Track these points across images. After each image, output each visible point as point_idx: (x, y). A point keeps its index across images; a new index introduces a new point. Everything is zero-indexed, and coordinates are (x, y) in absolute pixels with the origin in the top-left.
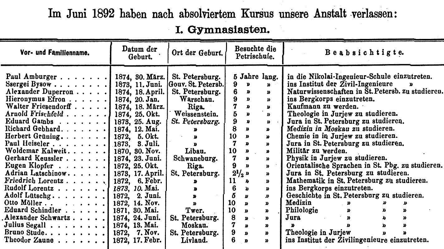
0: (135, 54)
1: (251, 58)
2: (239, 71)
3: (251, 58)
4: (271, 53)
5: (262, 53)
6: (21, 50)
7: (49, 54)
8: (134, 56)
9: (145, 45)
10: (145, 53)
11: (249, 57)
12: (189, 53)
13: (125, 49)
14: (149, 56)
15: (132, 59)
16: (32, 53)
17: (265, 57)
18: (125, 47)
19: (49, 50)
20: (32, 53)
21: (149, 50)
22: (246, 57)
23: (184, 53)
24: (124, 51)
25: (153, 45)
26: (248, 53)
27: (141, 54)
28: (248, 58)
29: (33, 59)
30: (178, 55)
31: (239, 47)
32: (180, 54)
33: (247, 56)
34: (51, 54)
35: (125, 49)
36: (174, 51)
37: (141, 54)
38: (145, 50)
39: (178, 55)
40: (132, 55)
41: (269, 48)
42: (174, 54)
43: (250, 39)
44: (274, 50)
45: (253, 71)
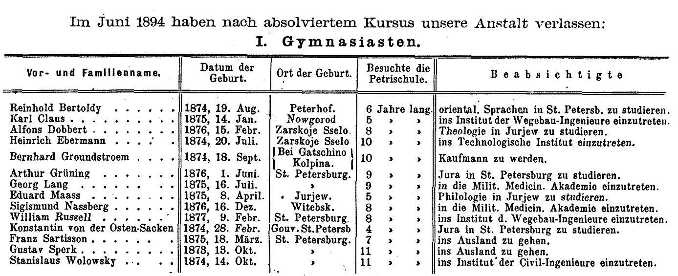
0: (219, 74)
1: (392, 82)
2: (375, 101)
6: (28, 70)
7: (84, 75)
8: (217, 77)
9: (235, 63)
10: (236, 72)
11: (389, 80)
12: (301, 73)
13: (204, 67)
14: (241, 77)
15: (215, 81)
16: (47, 74)
18: (205, 65)
19: (84, 70)
20: (47, 74)
21: (242, 67)
22: (384, 80)
24: (202, 70)
25: (247, 62)
26: (387, 74)
27: (228, 74)
30: (286, 76)
32: (288, 74)
33: (385, 79)
34: (86, 75)
35: (205, 68)
36: (280, 71)
37: (228, 74)
39: (286, 76)
40: (215, 75)
42: (280, 74)
43: (393, 61)
45: (397, 101)
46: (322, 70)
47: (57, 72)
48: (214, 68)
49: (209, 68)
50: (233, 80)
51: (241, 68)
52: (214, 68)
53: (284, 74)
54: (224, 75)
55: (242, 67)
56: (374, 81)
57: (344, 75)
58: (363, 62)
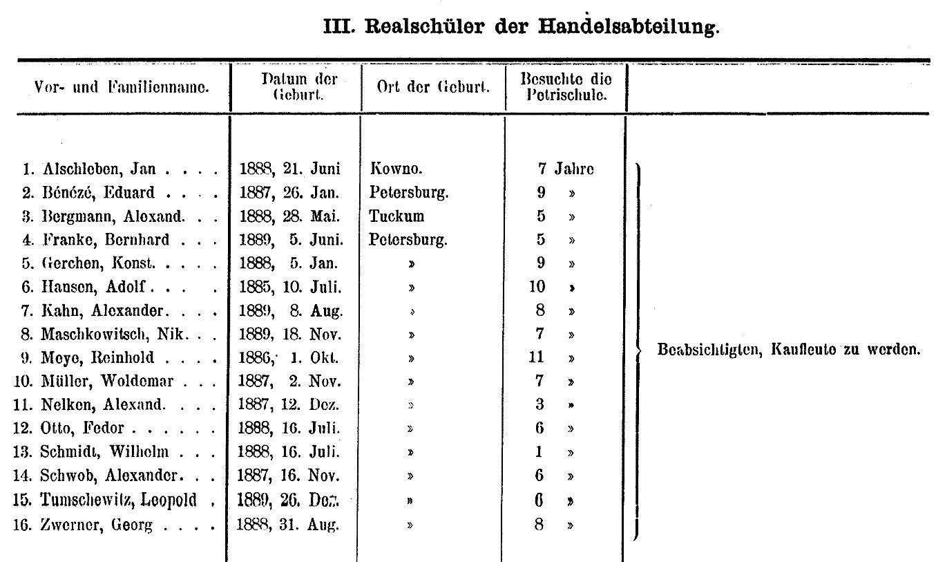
0: (287, 88)
3: (558, 99)
4: (598, 88)
5: (582, 89)
9: (311, 70)
10: (311, 86)
12: (412, 87)
16: (62, 88)
17: (587, 97)
20: (62, 88)
23: (403, 86)
26: (553, 88)
27: (300, 88)
28: (552, 99)
29: (67, 100)
32: (393, 88)
33: (549, 95)
36: (382, 84)
37: (300, 88)
41: (594, 79)
44: (607, 80)
47: (75, 85)
50: (304, 96)
54: (294, 90)
56: (534, 97)
57: (479, 88)
58: (515, 70)
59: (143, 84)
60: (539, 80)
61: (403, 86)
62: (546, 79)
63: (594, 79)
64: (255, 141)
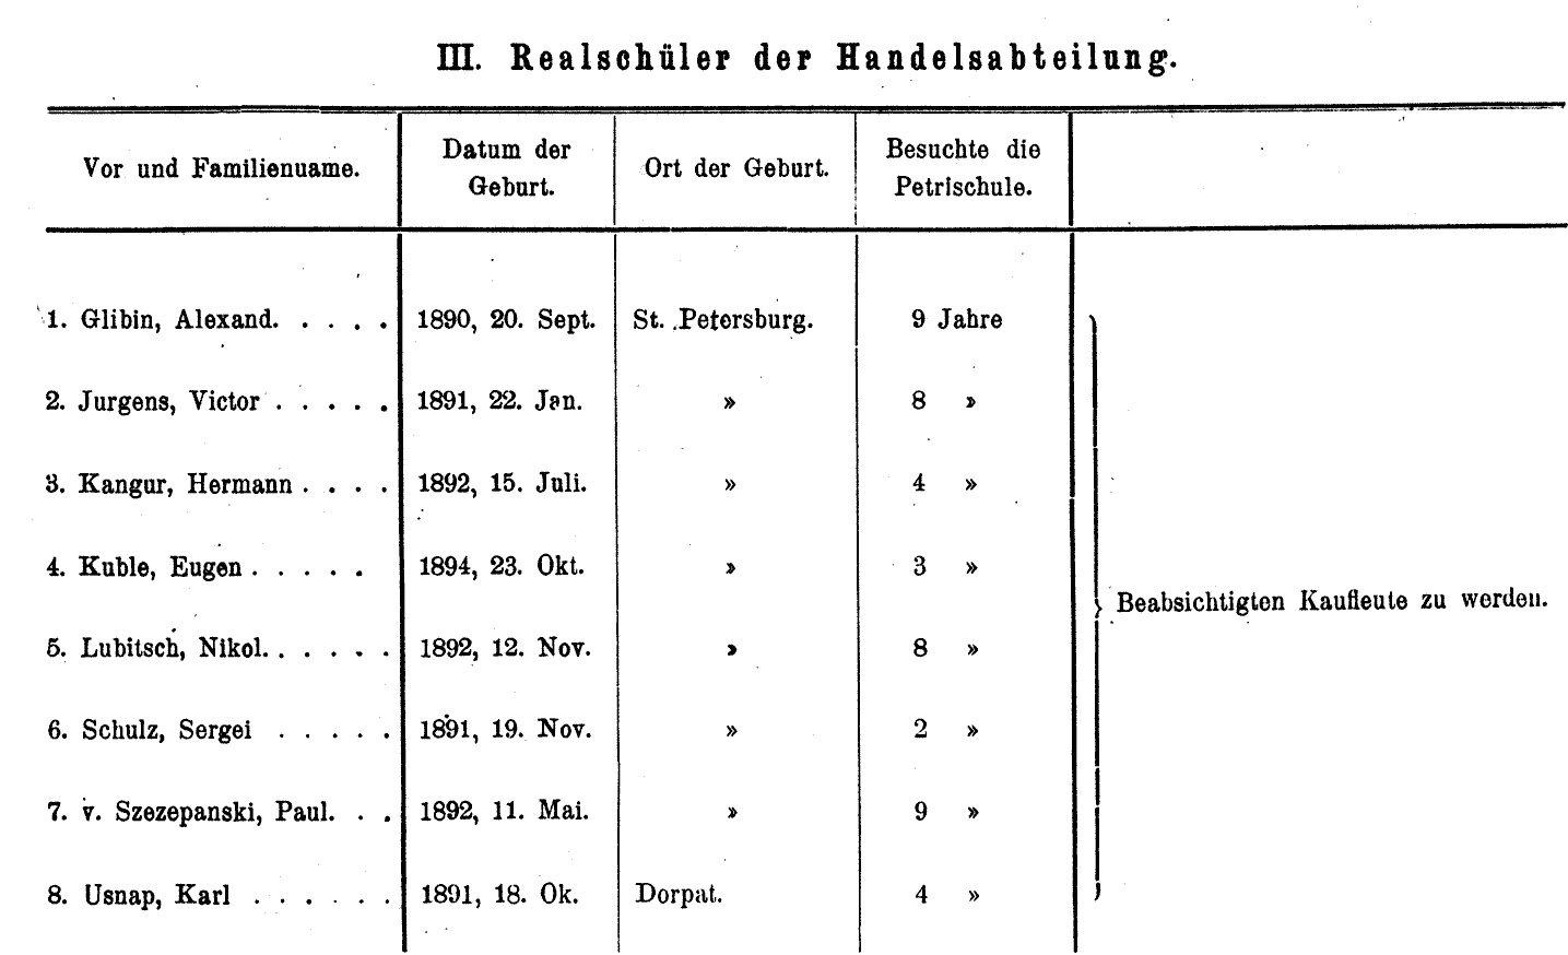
21: (546, 151)
23: (687, 168)
24: (448, 156)
31: (900, 142)
32: (671, 171)
35: (453, 151)
36: (653, 164)
38: (528, 151)
39: (666, 175)
42: (653, 169)
44: (1035, 151)
46: (758, 161)
48: (477, 150)
49: (463, 151)
51: (541, 153)
52: (477, 150)
53: (663, 172)
55: (546, 151)
59: (250, 164)
60: (916, 151)
61: (687, 168)
62: (927, 150)
63: (1012, 149)
64: (440, 274)
